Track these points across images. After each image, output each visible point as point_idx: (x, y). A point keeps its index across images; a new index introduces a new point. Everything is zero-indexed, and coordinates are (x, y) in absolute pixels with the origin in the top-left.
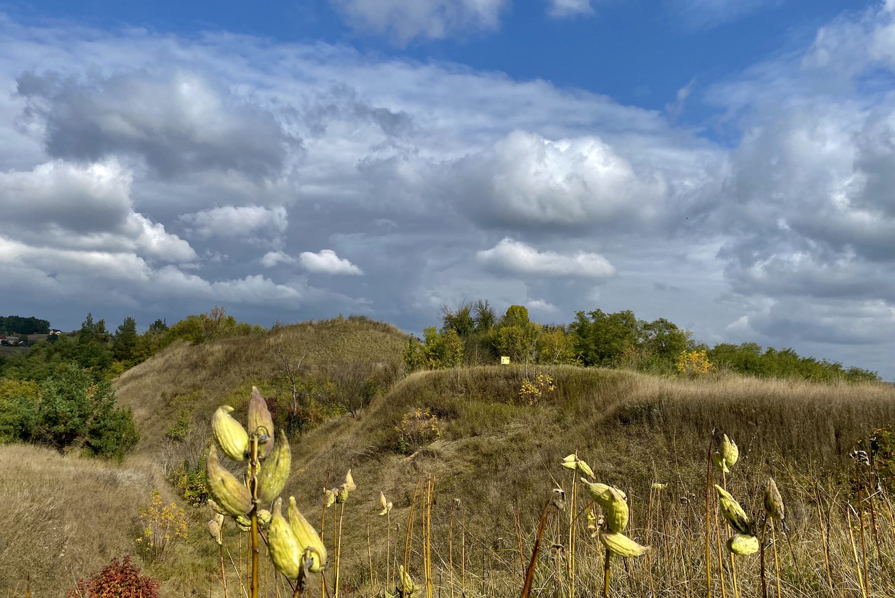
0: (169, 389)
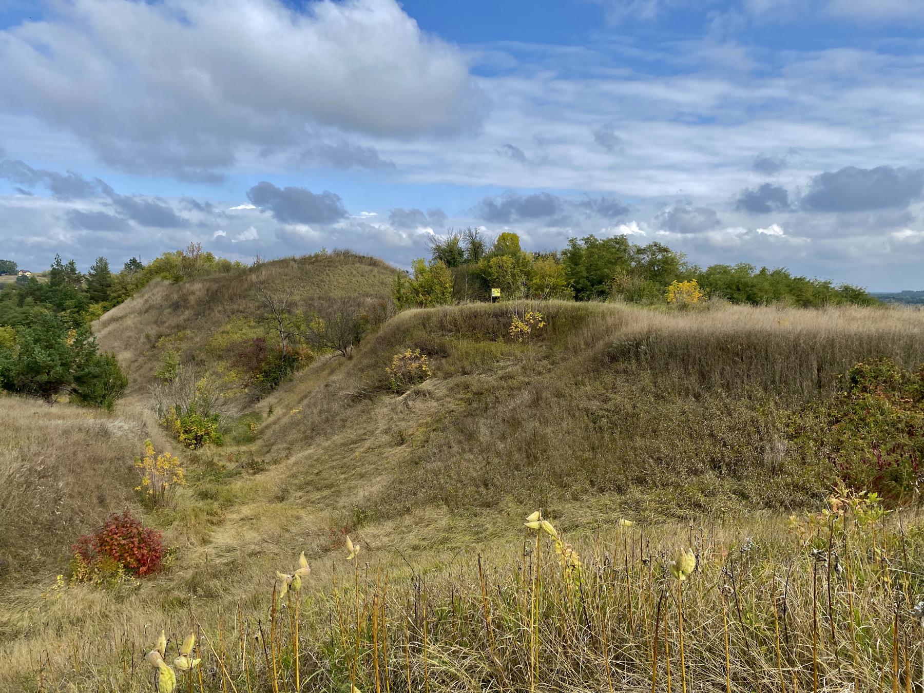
0: (153, 331)
